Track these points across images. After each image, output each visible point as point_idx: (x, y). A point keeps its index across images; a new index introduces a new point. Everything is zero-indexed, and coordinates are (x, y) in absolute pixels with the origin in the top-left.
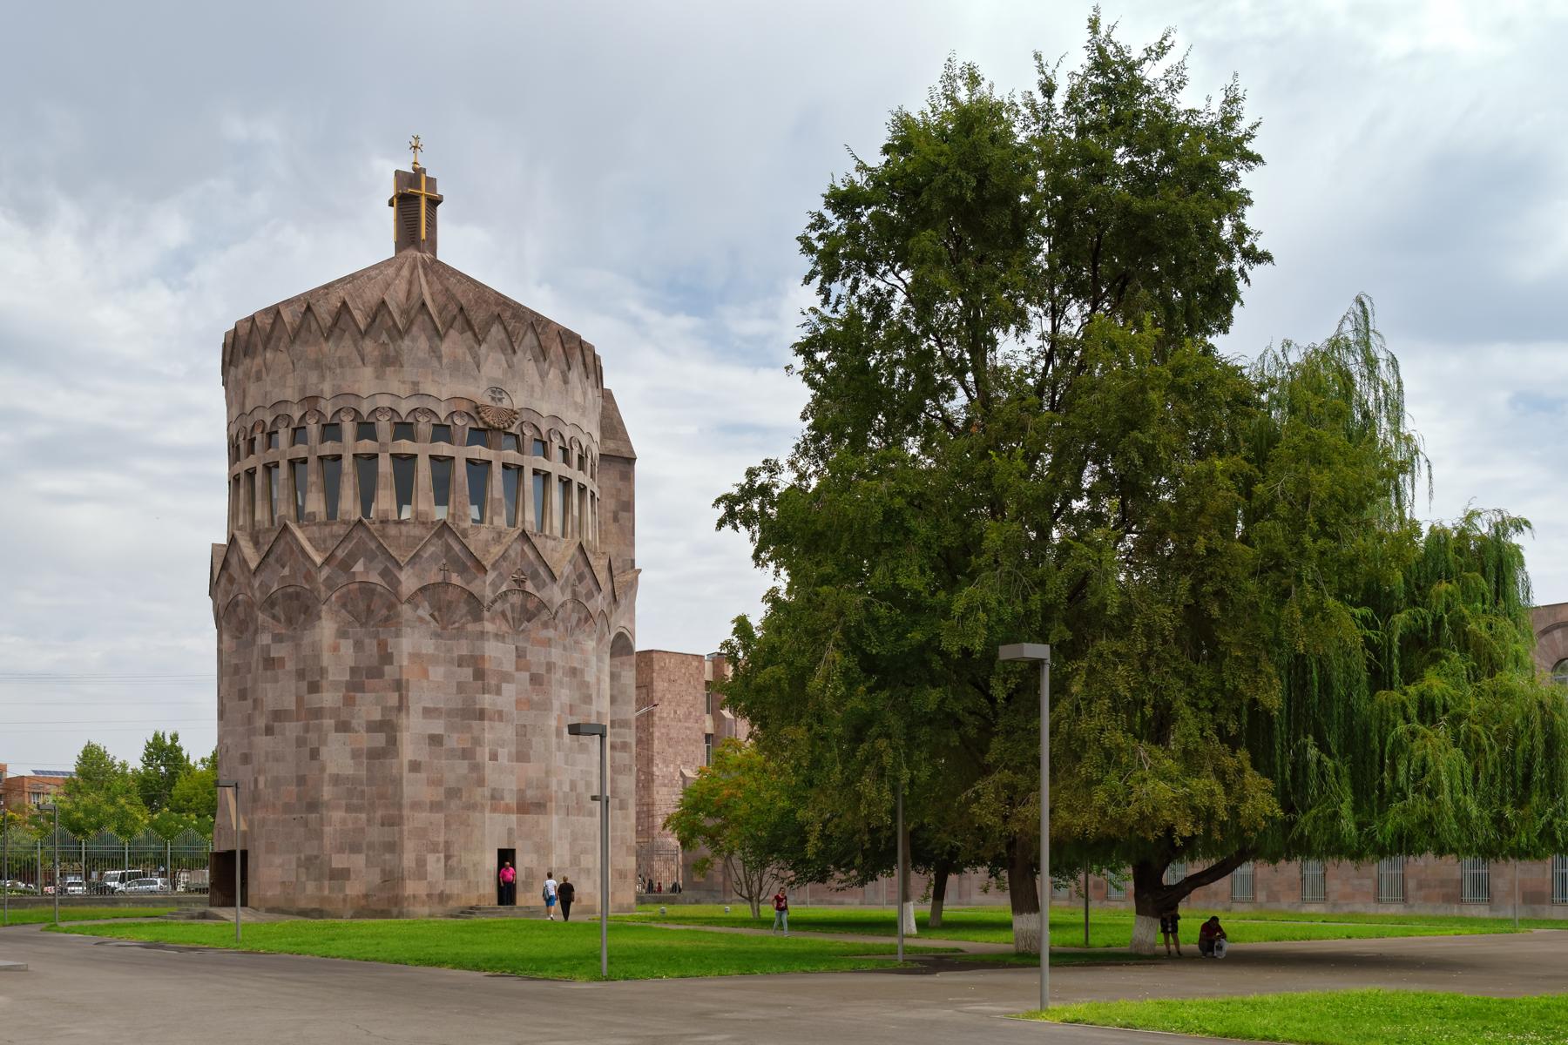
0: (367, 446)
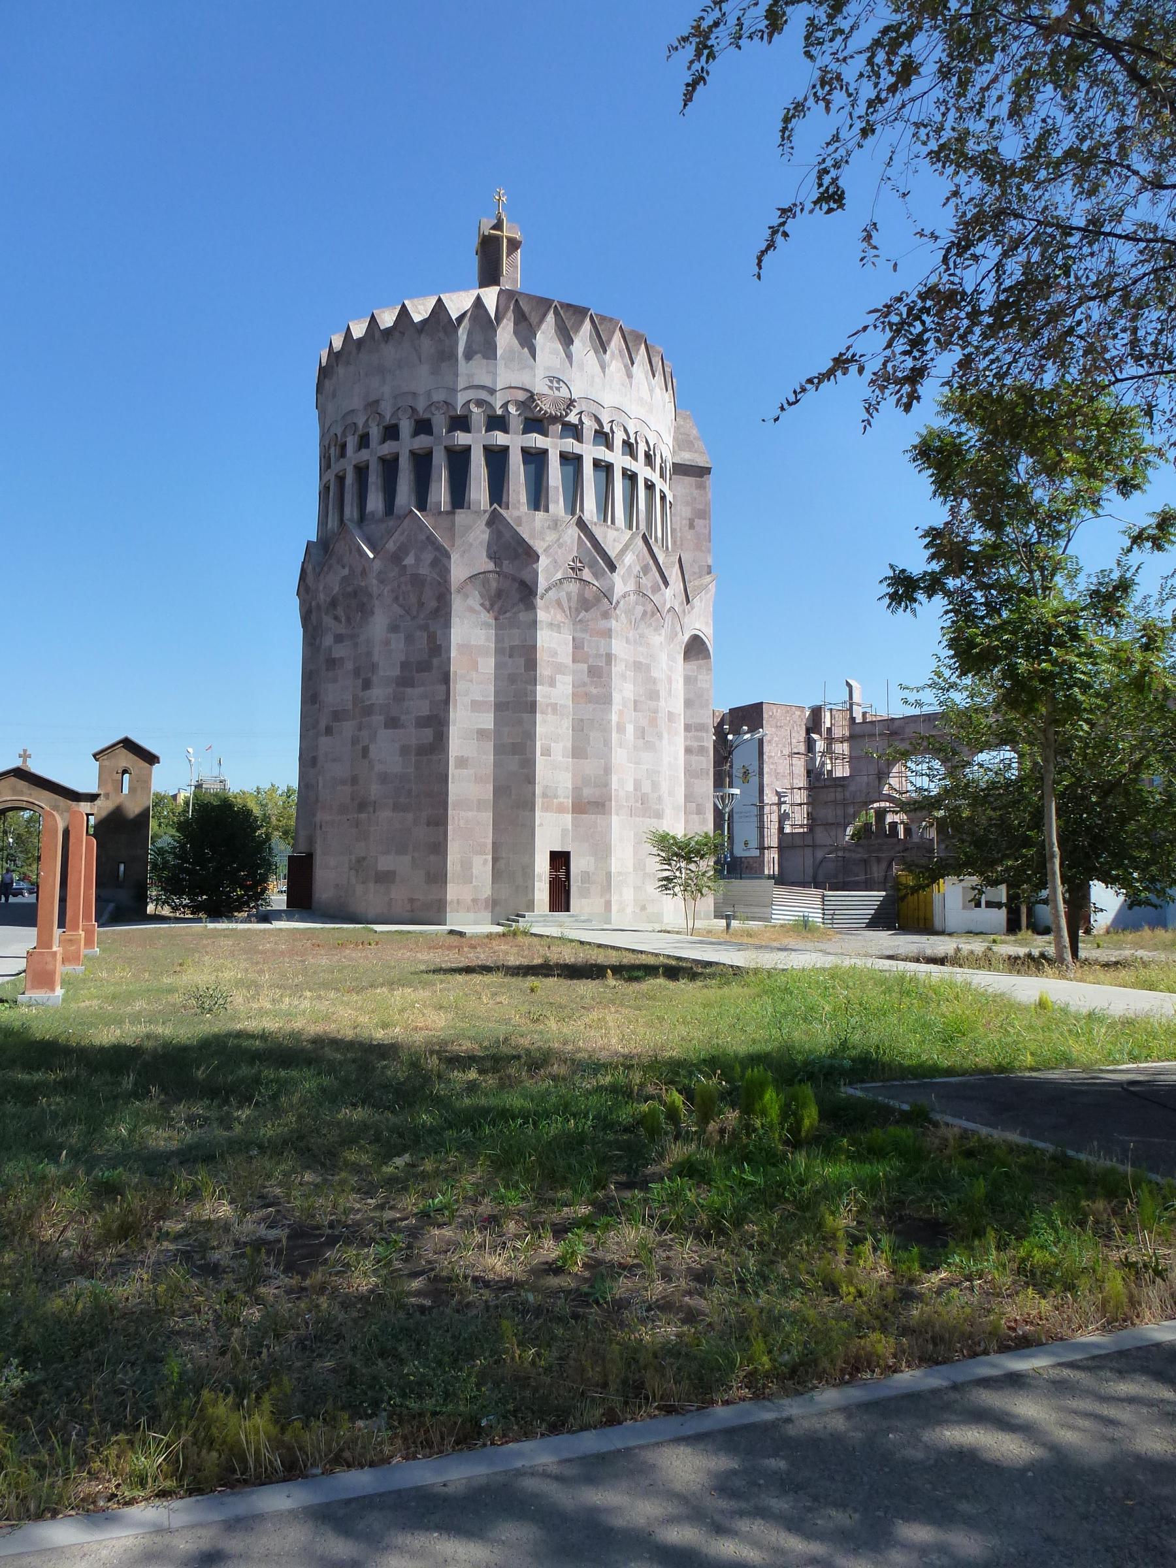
0: (422, 441)
